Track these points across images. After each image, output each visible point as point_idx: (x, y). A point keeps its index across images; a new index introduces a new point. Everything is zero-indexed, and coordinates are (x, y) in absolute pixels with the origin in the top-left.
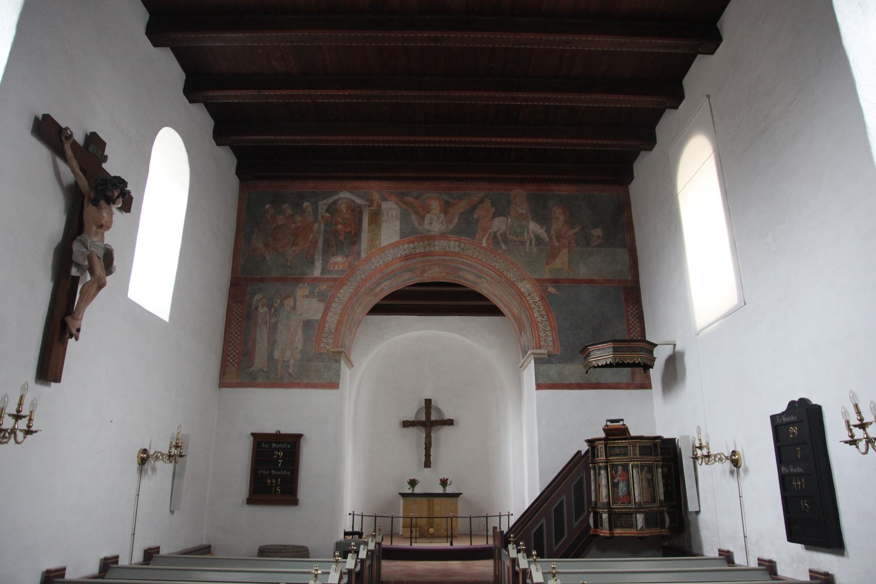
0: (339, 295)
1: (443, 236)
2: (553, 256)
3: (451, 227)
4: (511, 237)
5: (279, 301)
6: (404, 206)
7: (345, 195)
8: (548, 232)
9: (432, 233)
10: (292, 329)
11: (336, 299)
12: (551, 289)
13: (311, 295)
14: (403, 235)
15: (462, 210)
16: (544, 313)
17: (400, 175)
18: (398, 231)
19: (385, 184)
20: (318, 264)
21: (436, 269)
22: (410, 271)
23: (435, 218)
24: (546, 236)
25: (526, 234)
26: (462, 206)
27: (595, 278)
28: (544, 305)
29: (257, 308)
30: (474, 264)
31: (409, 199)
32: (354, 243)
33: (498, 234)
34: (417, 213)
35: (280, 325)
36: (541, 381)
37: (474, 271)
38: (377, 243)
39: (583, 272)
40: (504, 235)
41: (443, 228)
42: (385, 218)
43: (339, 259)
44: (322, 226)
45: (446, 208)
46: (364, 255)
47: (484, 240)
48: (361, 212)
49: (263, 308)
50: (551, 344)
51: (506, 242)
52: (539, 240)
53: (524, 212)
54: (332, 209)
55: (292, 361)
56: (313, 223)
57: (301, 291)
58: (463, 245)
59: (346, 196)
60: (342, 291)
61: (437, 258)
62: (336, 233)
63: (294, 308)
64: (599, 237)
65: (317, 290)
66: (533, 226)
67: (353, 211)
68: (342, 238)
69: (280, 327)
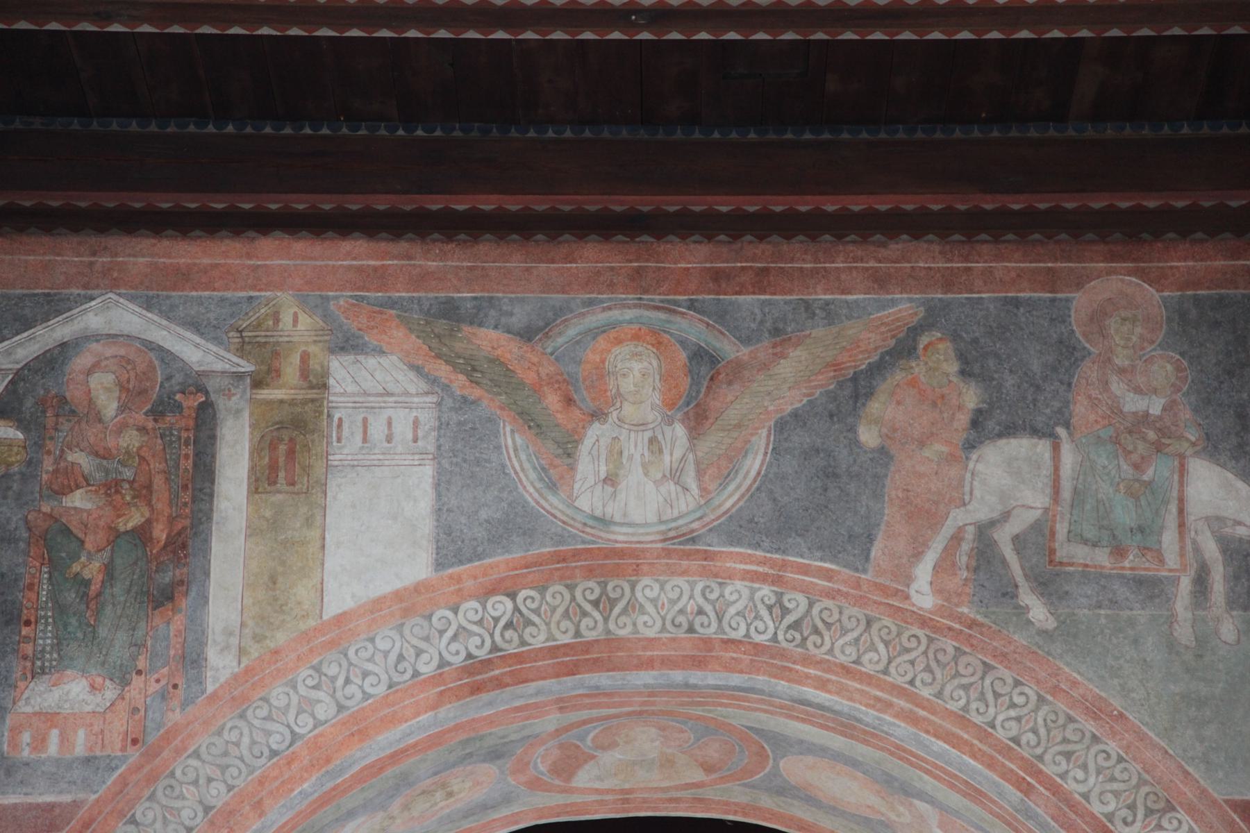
1: (683, 548)
3: (730, 499)
4: (1081, 553)
6: (459, 382)
7: (112, 317)
9: (620, 537)
14: (451, 548)
15: (792, 401)
17: (435, 204)
18: (427, 526)
19: (352, 254)
21: (646, 740)
22: (495, 755)
23: (635, 446)
25: (1169, 539)
26: (788, 381)
30: (870, 715)
31: (487, 340)
32: (163, 598)
33: (1003, 537)
34: (531, 422)
37: (861, 751)
38: (303, 592)
40: (1037, 541)
41: (686, 503)
42: (346, 449)
45: (700, 388)
46: (221, 665)
47: (923, 572)
51: (1049, 581)
58: (797, 602)
61: (645, 678)
67: (157, 413)
68: (91, 569)
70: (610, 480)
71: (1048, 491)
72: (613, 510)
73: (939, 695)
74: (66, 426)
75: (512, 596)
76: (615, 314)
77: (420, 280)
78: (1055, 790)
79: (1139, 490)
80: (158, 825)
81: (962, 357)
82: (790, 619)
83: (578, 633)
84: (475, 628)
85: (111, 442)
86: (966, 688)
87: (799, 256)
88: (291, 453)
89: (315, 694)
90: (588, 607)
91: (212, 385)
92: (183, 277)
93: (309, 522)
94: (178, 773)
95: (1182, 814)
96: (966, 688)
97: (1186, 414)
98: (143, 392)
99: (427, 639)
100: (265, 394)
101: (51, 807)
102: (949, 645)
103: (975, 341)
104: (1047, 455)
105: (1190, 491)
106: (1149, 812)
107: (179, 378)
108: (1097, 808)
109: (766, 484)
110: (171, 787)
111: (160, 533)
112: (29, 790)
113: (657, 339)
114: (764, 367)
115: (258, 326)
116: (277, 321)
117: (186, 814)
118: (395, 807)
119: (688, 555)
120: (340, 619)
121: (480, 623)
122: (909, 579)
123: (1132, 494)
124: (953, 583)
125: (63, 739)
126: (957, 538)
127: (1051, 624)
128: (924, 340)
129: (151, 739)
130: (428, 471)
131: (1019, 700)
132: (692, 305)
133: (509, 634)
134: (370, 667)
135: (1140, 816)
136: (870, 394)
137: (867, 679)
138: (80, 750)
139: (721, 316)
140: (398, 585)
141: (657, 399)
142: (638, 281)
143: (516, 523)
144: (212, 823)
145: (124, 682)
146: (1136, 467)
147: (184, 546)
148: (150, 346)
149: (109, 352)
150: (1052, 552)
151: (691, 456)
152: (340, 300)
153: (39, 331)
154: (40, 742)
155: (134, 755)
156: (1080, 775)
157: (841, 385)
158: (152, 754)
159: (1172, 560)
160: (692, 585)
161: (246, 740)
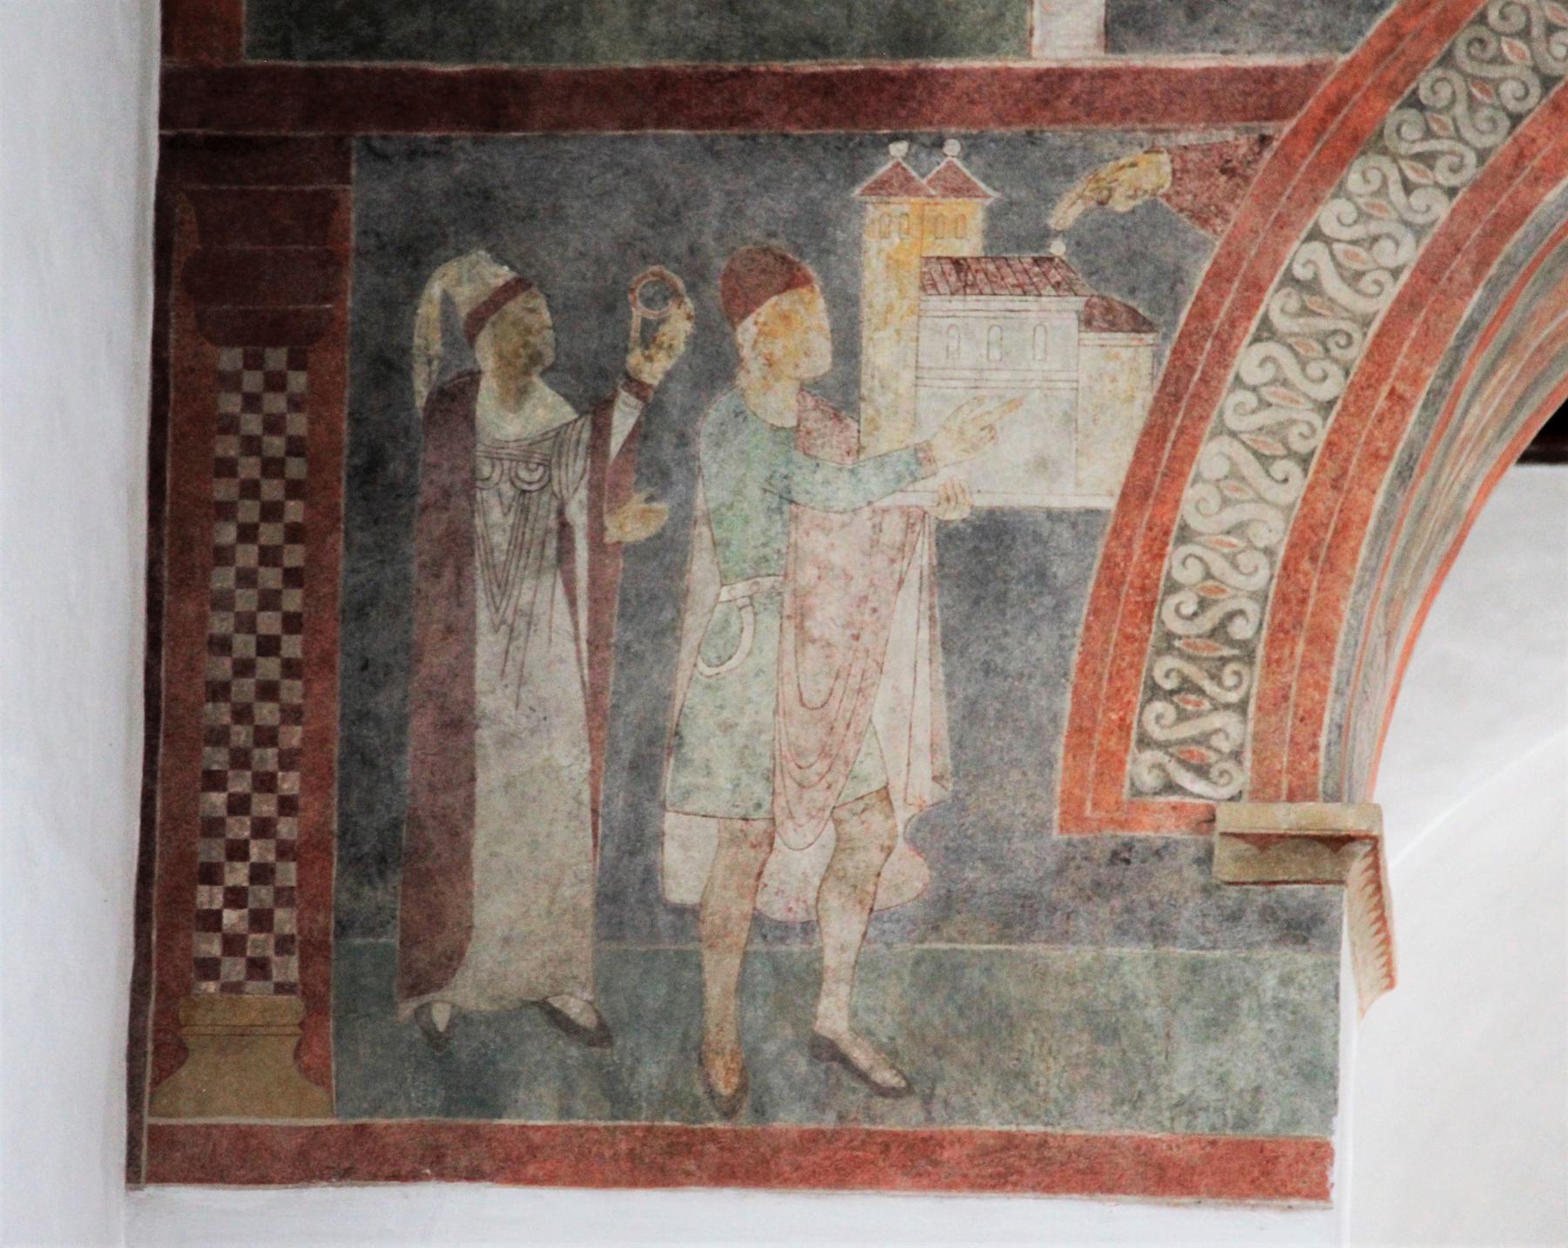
0: (1304, 258)
5: (678, 326)
10: (828, 614)
11: (1277, 305)
13: (1013, 258)
29: (456, 397)
35: (701, 567)
49: (517, 395)
57: (908, 219)
60: (1332, 214)
63: (841, 394)
65: (1066, 212)
69: (709, 589)
80: (1460, 109)
94: (1493, 15)
101: (1270, 75)
110: (1481, 41)
112: (1230, 45)
117: (1509, 90)
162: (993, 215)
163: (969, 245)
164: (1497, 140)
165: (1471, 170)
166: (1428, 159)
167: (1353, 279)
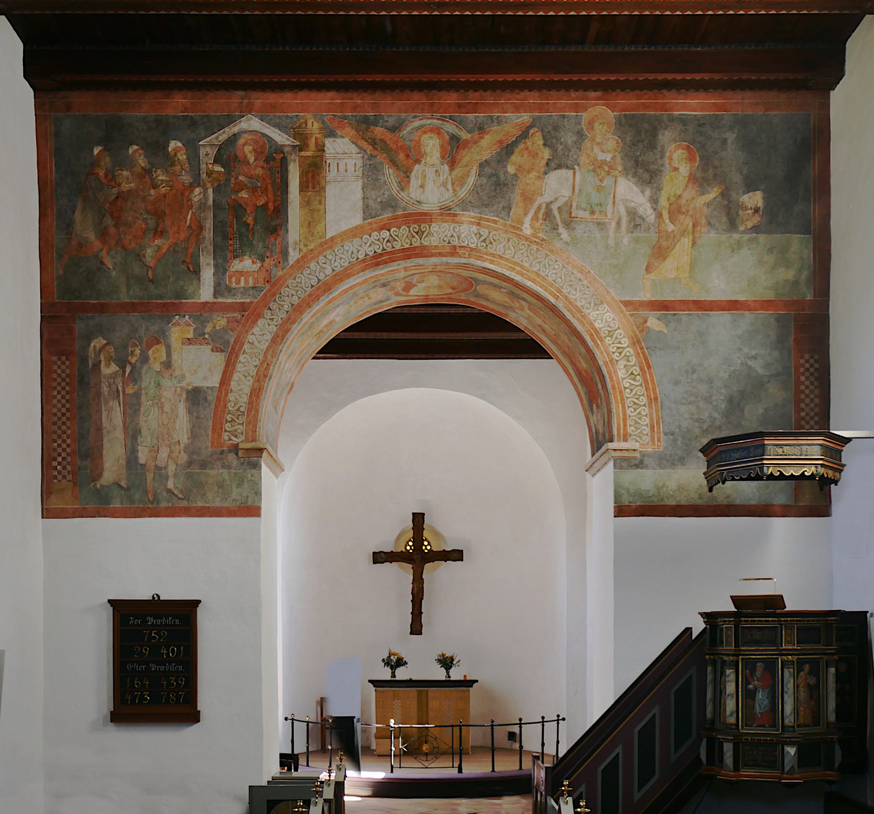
1: (447, 213)
2: (660, 252)
3: (463, 193)
5: (138, 352)
6: (369, 149)
8: (654, 201)
9: (425, 208)
10: (167, 408)
11: (246, 347)
12: (654, 322)
13: (198, 338)
14: (367, 212)
15: (486, 156)
16: (637, 370)
20: (208, 274)
23: (430, 173)
24: (650, 211)
25: (609, 208)
26: (486, 147)
27: (741, 298)
28: (637, 355)
29: (97, 365)
33: (554, 207)
34: (394, 163)
35: (143, 398)
36: (626, 500)
38: (320, 228)
39: (718, 287)
42: (331, 175)
43: (246, 263)
44: (210, 191)
45: (453, 151)
46: (294, 256)
47: (527, 220)
48: (284, 164)
49: (108, 365)
50: (648, 430)
52: (635, 220)
53: (608, 157)
54: (227, 155)
55: (172, 468)
56: (191, 187)
57: (179, 331)
59: (254, 126)
60: (256, 330)
61: (434, 260)
62: (238, 209)
63: (168, 365)
64: (756, 210)
65: (208, 329)
66: (628, 191)
67: (267, 161)
68: (250, 220)
69: (146, 403)
70: (422, 186)
71: (571, 190)
72: (422, 198)
73: (531, 265)
74: (237, 166)
75: (389, 230)
76: (424, 122)
77: (355, 108)
78: (566, 298)
79: (599, 189)
81: (544, 138)
82: (482, 238)
83: (411, 244)
84: (377, 242)
85: (252, 172)
86: (539, 262)
87: (489, 98)
88: (313, 177)
89: (324, 266)
90: (415, 234)
91: (287, 149)
92: (274, 107)
93: (320, 203)
95: (605, 305)
96: (539, 262)
97: (619, 160)
98: (262, 153)
99: (361, 246)
100: (303, 154)
102: (535, 247)
103: (549, 132)
104: (571, 177)
105: (618, 190)
106: (596, 304)
107: (274, 147)
108: (579, 304)
109: (475, 190)
111: (271, 206)
113: (437, 131)
114: (476, 142)
115: (300, 127)
116: (306, 125)
117: (286, 307)
118: (352, 302)
119: (449, 215)
120: (332, 239)
121: (378, 240)
122: (522, 223)
123: (598, 191)
124: (537, 225)
125: (246, 281)
126: (539, 208)
127: (568, 239)
128: (531, 131)
129: (273, 280)
130: (360, 183)
131: (556, 267)
132: (451, 118)
133: (388, 244)
134: (342, 256)
135: (592, 305)
136: (512, 153)
137: (507, 260)
138: (251, 284)
139: (461, 123)
140: (351, 226)
141: (438, 155)
142: (432, 109)
143: (390, 204)
144: (294, 310)
145: (263, 261)
146: (601, 181)
147: (279, 212)
148: (264, 135)
149: (250, 137)
150: (571, 213)
151: (450, 178)
152: (327, 117)
153: (226, 129)
154: (238, 281)
155: (268, 287)
156: (574, 292)
157: (502, 149)
158: (273, 286)
159: (609, 215)
160: (450, 226)
161: (303, 282)
162: (195, 330)
163: (190, 336)
164: (284, 316)
165: (280, 321)
166: (272, 319)
167: (260, 342)
